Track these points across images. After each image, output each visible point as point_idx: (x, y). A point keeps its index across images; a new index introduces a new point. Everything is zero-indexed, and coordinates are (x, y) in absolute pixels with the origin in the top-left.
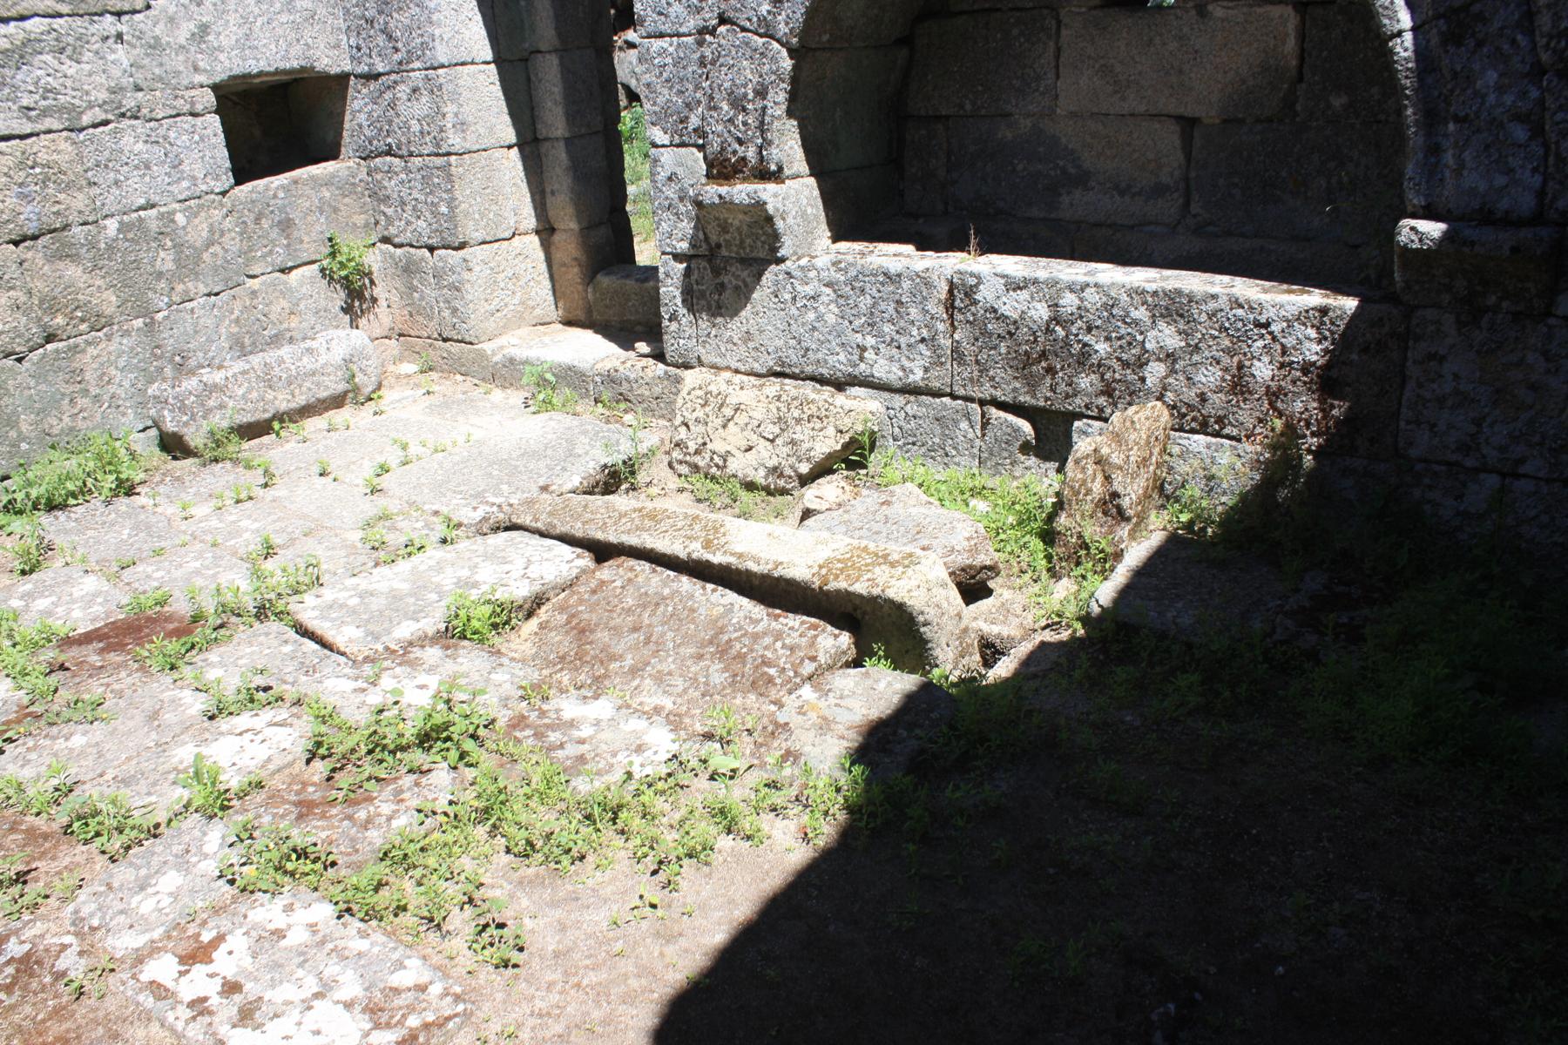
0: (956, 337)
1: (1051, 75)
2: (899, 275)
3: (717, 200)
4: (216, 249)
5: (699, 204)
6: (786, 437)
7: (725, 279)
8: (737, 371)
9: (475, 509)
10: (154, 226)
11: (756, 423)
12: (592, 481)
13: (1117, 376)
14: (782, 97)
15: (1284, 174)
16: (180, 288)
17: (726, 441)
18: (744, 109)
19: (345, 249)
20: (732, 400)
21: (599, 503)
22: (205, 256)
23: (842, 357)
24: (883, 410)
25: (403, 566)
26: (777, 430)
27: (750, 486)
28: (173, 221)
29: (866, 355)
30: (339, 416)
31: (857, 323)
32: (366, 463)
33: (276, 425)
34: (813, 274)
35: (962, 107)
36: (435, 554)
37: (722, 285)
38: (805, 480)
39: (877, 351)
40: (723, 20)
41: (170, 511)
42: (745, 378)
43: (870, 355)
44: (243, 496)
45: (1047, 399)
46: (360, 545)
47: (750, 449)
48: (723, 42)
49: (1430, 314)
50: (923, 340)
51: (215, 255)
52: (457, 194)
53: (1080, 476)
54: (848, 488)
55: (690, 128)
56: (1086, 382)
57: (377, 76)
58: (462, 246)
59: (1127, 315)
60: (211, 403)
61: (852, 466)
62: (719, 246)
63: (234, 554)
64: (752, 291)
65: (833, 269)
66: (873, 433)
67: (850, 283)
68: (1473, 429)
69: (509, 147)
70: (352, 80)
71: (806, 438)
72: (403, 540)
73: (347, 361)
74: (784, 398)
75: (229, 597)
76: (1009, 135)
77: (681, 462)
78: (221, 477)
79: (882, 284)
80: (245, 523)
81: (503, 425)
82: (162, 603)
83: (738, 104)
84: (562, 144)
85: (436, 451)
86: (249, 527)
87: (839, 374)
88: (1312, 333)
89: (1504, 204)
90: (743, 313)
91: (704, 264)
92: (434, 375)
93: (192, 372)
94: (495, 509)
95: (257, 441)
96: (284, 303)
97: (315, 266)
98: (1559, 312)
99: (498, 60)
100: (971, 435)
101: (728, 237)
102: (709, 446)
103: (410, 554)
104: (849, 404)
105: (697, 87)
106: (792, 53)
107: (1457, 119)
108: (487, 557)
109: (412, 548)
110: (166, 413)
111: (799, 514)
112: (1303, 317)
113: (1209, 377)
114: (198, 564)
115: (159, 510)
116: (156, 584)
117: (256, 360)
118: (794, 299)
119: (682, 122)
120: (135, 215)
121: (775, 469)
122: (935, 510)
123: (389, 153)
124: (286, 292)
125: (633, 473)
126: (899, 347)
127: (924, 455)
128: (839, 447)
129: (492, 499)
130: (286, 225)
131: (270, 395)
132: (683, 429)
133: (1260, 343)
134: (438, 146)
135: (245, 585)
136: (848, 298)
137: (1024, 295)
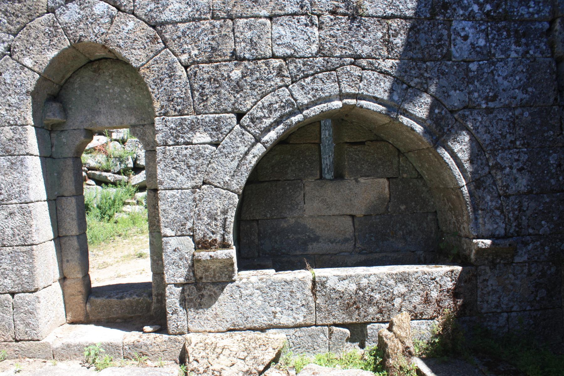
1: (302, 203)
2: (292, 281)
3: (209, 258)
6: (251, 356)
7: (204, 292)
8: (210, 332)
13: (384, 306)
15: (388, 231)
18: (216, 219)
23: (265, 318)
24: (285, 337)
26: (246, 354)
31: (272, 303)
35: (265, 215)
37: (203, 295)
39: (282, 313)
40: (204, 183)
45: (356, 319)
47: (233, 365)
48: (205, 192)
49: (482, 267)
50: (303, 305)
52: (35, 264)
53: (393, 344)
55: (187, 228)
56: (372, 310)
59: (387, 283)
62: (201, 278)
68: (498, 300)
69: (51, 240)
71: (260, 355)
74: (246, 339)
76: (286, 225)
83: (213, 217)
84: (75, 238)
88: (449, 279)
89: (497, 233)
90: (214, 306)
98: (515, 262)
99: (48, 200)
102: (211, 368)
105: (191, 211)
107: (482, 210)
112: (446, 274)
113: (417, 300)
119: (182, 225)
121: (247, 371)
126: (292, 310)
133: (433, 285)
134: (25, 241)
137: (346, 282)
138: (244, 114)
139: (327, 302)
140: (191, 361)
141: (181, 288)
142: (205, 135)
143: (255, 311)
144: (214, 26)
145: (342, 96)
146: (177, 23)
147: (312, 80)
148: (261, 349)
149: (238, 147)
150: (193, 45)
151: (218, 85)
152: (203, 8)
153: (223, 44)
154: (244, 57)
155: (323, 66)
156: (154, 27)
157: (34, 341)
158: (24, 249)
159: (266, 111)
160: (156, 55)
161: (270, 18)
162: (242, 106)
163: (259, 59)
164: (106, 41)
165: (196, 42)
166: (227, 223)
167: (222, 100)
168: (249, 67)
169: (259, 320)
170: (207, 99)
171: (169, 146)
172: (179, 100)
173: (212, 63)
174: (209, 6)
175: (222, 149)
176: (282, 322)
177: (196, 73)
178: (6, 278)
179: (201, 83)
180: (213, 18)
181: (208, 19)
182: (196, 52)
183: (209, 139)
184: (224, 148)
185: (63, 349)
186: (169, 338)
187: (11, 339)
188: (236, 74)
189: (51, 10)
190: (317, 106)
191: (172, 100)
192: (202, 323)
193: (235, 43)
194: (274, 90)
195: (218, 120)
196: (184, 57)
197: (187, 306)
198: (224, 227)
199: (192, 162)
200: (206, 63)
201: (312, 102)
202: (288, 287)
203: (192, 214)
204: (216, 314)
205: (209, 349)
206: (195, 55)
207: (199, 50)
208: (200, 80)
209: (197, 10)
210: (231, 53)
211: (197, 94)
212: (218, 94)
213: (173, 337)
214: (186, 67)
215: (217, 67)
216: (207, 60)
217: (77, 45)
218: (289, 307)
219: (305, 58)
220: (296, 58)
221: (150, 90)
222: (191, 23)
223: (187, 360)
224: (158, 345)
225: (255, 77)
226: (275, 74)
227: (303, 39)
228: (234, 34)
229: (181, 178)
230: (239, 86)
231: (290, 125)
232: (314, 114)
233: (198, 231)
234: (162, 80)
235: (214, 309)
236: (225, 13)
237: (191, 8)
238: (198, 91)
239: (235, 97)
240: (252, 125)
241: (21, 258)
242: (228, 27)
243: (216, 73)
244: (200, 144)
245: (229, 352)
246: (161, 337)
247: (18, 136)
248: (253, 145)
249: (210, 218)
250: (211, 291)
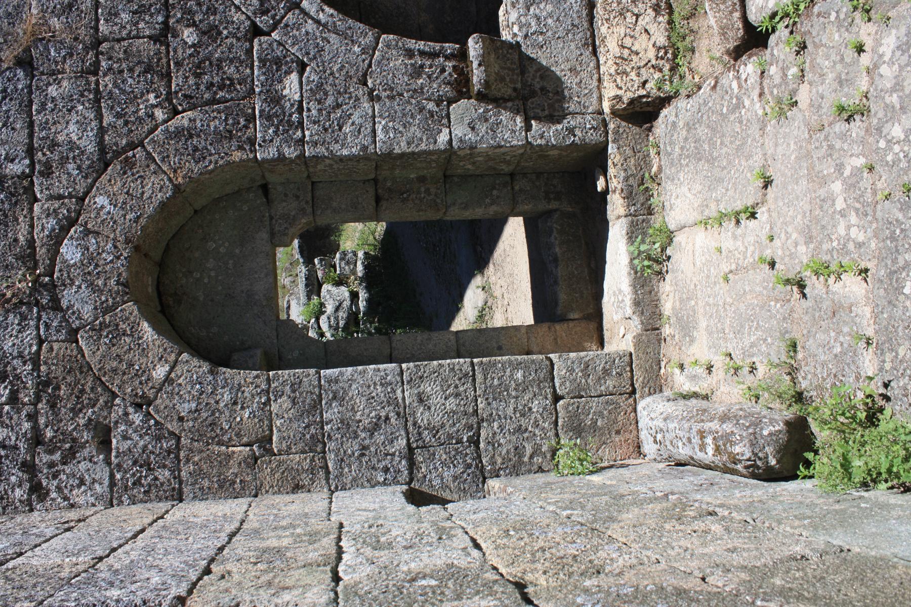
3: (483, 68)
17: (646, 48)
18: (422, 66)
26: (629, 14)
27: (670, 22)
34: (523, 20)
47: (646, 31)
48: (378, 81)
57: (411, 450)
62: (515, 89)
70: (415, 485)
74: (607, 16)
83: (417, 72)
90: (558, 73)
102: (653, 62)
105: (409, 102)
110: (765, 433)
118: (542, 33)
119: (432, 116)
121: (655, 10)
123: (477, 443)
134: (466, 375)
138: (254, 24)
140: (645, 93)
141: (533, 122)
142: (287, 82)
143: (563, 14)
144: (110, 69)
149: (307, 33)
150: (139, 101)
151: (207, 63)
152: (79, 86)
153: (140, 56)
154: (162, 23)
157: (632, 363)
158: (479, 377)
162: (242, 26)
164: (127, 241)
165: (136, 97)
166: (427, 49)
167: (231, 56)
168: (179, 16)
169: (576, 9)
170: (229, 79)
171: (304, 136)
172: (230, 121)
173: (170, 73)
174: (76, 77)
175: (311, 56)
177: (185, 96)
178: (530, 409)
179: (202, 87)
180: (95, 73)
183: (294, 76)
184: (308, 54)
185: (642, 313)
186: (613, 142)
187: (631, 400)
188: (189, 35)
191: (230, 132)
192: (587, 91)
193: (139, 38)
195: (263, 61)
196: (159, 114)
197: (561, 113)
198: (433, 55)
199: (330, 101)
200: (170, 82)
203: (414, 101)
204: (571, 70)
205: (624, 66)
206: (156, 97)
207: (148, 92)
208: (198, 89)
209: (82, 95)
210: (155, 44)
211: (221, 94)
212: (221, 62)
213: (611, 137)
214: (176, 112)
215: (178, 64)
216: (165, 80)
222: (103, 105)
223: (644, 100)
224: (626, 160)
225: (195, 8)
228: (124, 39)
229: (356, 118)
230: (209, 31)
233: (441, 93)
234: (196, 149)
235: (563, 73)
236: (88, 53)
237: (78, 105)
238: (216, 93)
239: (227, 37)
241: (496, 382)
242: (112, 48)
243: (188, 64)
244: (301, 89)
245: (628, 38)
246: (612, 156)
249: (419, 76)
250: (534, 76)
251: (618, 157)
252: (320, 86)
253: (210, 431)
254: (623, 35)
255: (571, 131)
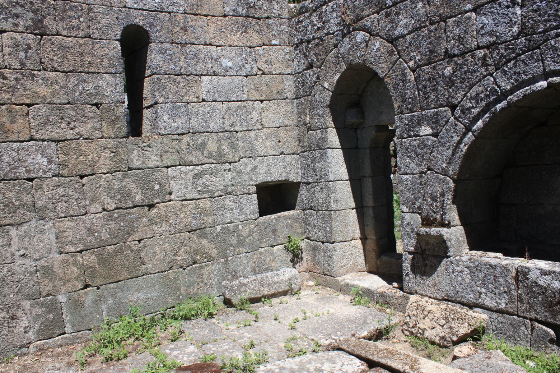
0: (519, 292)
2: (495, 266)
3: (425, 234)
4: (251, 237)
5: (418, 234)
8: (430, 297)
9: (327, 340)
10: (232, 229)
11: (436, 318)
12: (372, 334)
14: (450, 197)
16: (237, 250)
18: (436, 201)
19: (293, 241)
20: (428, 309)
21: (372, 344)
22: (247, 240)
23: (472, 296)
24: (488, 318)
25: (297, 359)
26: (444, 322)
27: (433, 343)
28: (238, 228)
29: (482, 296)
30: (285, 298)
32: (291, 317)
33: (263, 300)
34: (461, 263)
36: (309, 356)
37: (426, 264)
38: (455, 343)
40: (429, 169)
41: (222, 326)
42: (433, 300)
43: (483, 296)
44: (247, 324)
46: (283, 348)
47: (433, 328)
48: (429, 177)
50: (505, 292)
51: (250, 240)
52: (333, 224)
54: (472, 348)
55: (416, 207)
57: (310, 183)
58: (333, 242)
60: (242, 290)
61: (474, 340)
62: (425, 250)
63: (240, 345)
64: (437, 267)
65: (469, 262)
66: (484, 327)
67: (475, 267)
69: (353, 209)
70: (301, 184)
71: (456, 326)
72: (299, 349)
73: (290, 280)
74: (448, 310)
75: (235, 363)
77: (406, 330)
78: (241, 316)
79: (489, 269)
80: (246, 334)
81: (342, 308)
82: (213, 359)
83: (434, 199)
84: (371, 208)
85: (316, 316)
86: (247, 335)
87: (470, 302)
90: (434, 276)
91: (419, 256)
92: (320, 287)
93: (237, 278)
94: (334, 341)
95: (255, 304)
96: (271, 257)
97: (283, 246)
99: (351, 179)
100: (526, 333)
101: (429, 247)
103: (300, 355)
104: (474, 315)
105: (419, 192)
106: (454, 181)
108: (328, 360)
109: (302, 352)
111: (451, 357)
114: (227, 347)
115: (219, 325)
116: (212, 352)
117: (259, 276)
118: (453, 272)
120: (226, 225)
122: (510, 364)
123: (311, 209)
124: (272, 254)
125: (388, 333)
126: (495, 294)
127: (505, 339)
128: (469, 332)
129: (333, 337)
130: (274, 231)
131: (262, 289)
132: (408, 318)
134: (328, 208)
135: (240, 357)
136: (474, 273)
137: (549, 277)
138: (457, 106)
139: (528, 294)
142: (427, 128)
144: (431, 31)
145: (546, 75)
146: (405, 35)
147: (514, 64)
148: (458, 322)
149: (452, 137)
151: (435, 83)
154: (454, 54)
155: (525, 47)
156: (391, 43)
158: (328, 213)
159: (473, 101)
160: (394, 65)
161: (474, 10)
162: (454, 100)
163: (467, 53)
164: (364, 61)
169: (468, 296)
171: (405, 138)
176: (486, 304)
177: (419, 75)
181: (427, 26)
182: (419, 57)
183: (430, 131)
184: (442, 138)
186: (403, 295)
188: (449, 70)
189: (336, 46)
190: (521, 91)
191: (405, 101)
194: (480, 81)
195: (437, 114)
199: (419, 151)
200: (427, 65)
201: (515, 86)
202: (492, 271)
207: (421, 55)
209: (418, 21)
210: (444, 52)
211: (421, 93)
214: (414, 71)
215: (434, 67)
217: (351, 67)
218: (492, 291)
219: (506, 42)
220: (499, 44)
221: (392, 94)
225: (463, 70)
226: (480, 64)
227: (505, 22)
229: (412, 165)
231: (494, 113)
232: (516, 99)
234: (398, 85)
238: (422, 90)
239: (448, 92)
240: (463, 116)
244: (425, 136)
247: (323, 136)
248: (465, 135)
250: (432, 262)
251: (398, 295)
252: (426, 145)
253: (312, 107)
254: (435, 314)
255: (407, 275)
